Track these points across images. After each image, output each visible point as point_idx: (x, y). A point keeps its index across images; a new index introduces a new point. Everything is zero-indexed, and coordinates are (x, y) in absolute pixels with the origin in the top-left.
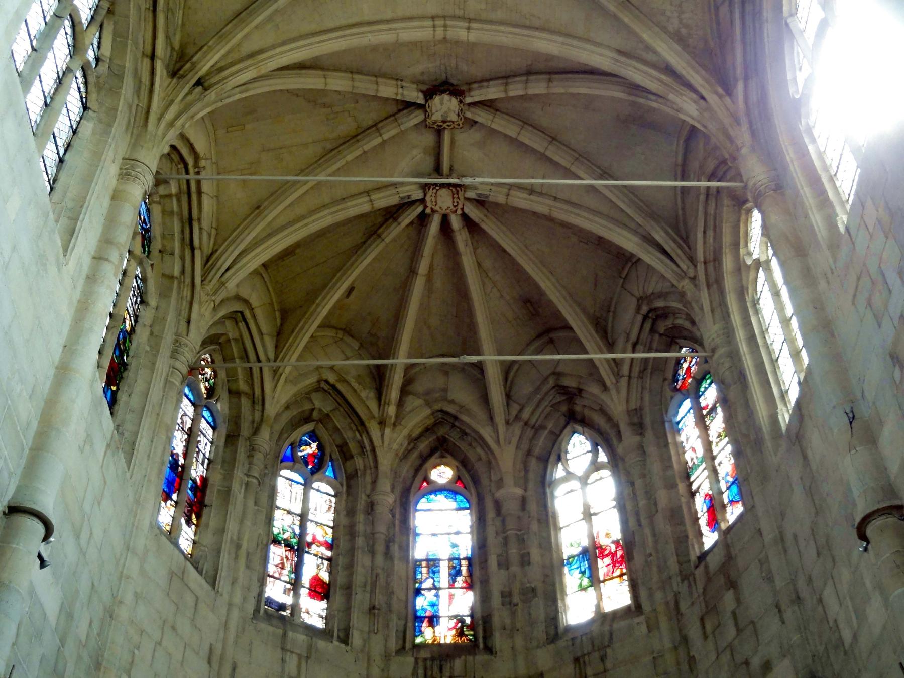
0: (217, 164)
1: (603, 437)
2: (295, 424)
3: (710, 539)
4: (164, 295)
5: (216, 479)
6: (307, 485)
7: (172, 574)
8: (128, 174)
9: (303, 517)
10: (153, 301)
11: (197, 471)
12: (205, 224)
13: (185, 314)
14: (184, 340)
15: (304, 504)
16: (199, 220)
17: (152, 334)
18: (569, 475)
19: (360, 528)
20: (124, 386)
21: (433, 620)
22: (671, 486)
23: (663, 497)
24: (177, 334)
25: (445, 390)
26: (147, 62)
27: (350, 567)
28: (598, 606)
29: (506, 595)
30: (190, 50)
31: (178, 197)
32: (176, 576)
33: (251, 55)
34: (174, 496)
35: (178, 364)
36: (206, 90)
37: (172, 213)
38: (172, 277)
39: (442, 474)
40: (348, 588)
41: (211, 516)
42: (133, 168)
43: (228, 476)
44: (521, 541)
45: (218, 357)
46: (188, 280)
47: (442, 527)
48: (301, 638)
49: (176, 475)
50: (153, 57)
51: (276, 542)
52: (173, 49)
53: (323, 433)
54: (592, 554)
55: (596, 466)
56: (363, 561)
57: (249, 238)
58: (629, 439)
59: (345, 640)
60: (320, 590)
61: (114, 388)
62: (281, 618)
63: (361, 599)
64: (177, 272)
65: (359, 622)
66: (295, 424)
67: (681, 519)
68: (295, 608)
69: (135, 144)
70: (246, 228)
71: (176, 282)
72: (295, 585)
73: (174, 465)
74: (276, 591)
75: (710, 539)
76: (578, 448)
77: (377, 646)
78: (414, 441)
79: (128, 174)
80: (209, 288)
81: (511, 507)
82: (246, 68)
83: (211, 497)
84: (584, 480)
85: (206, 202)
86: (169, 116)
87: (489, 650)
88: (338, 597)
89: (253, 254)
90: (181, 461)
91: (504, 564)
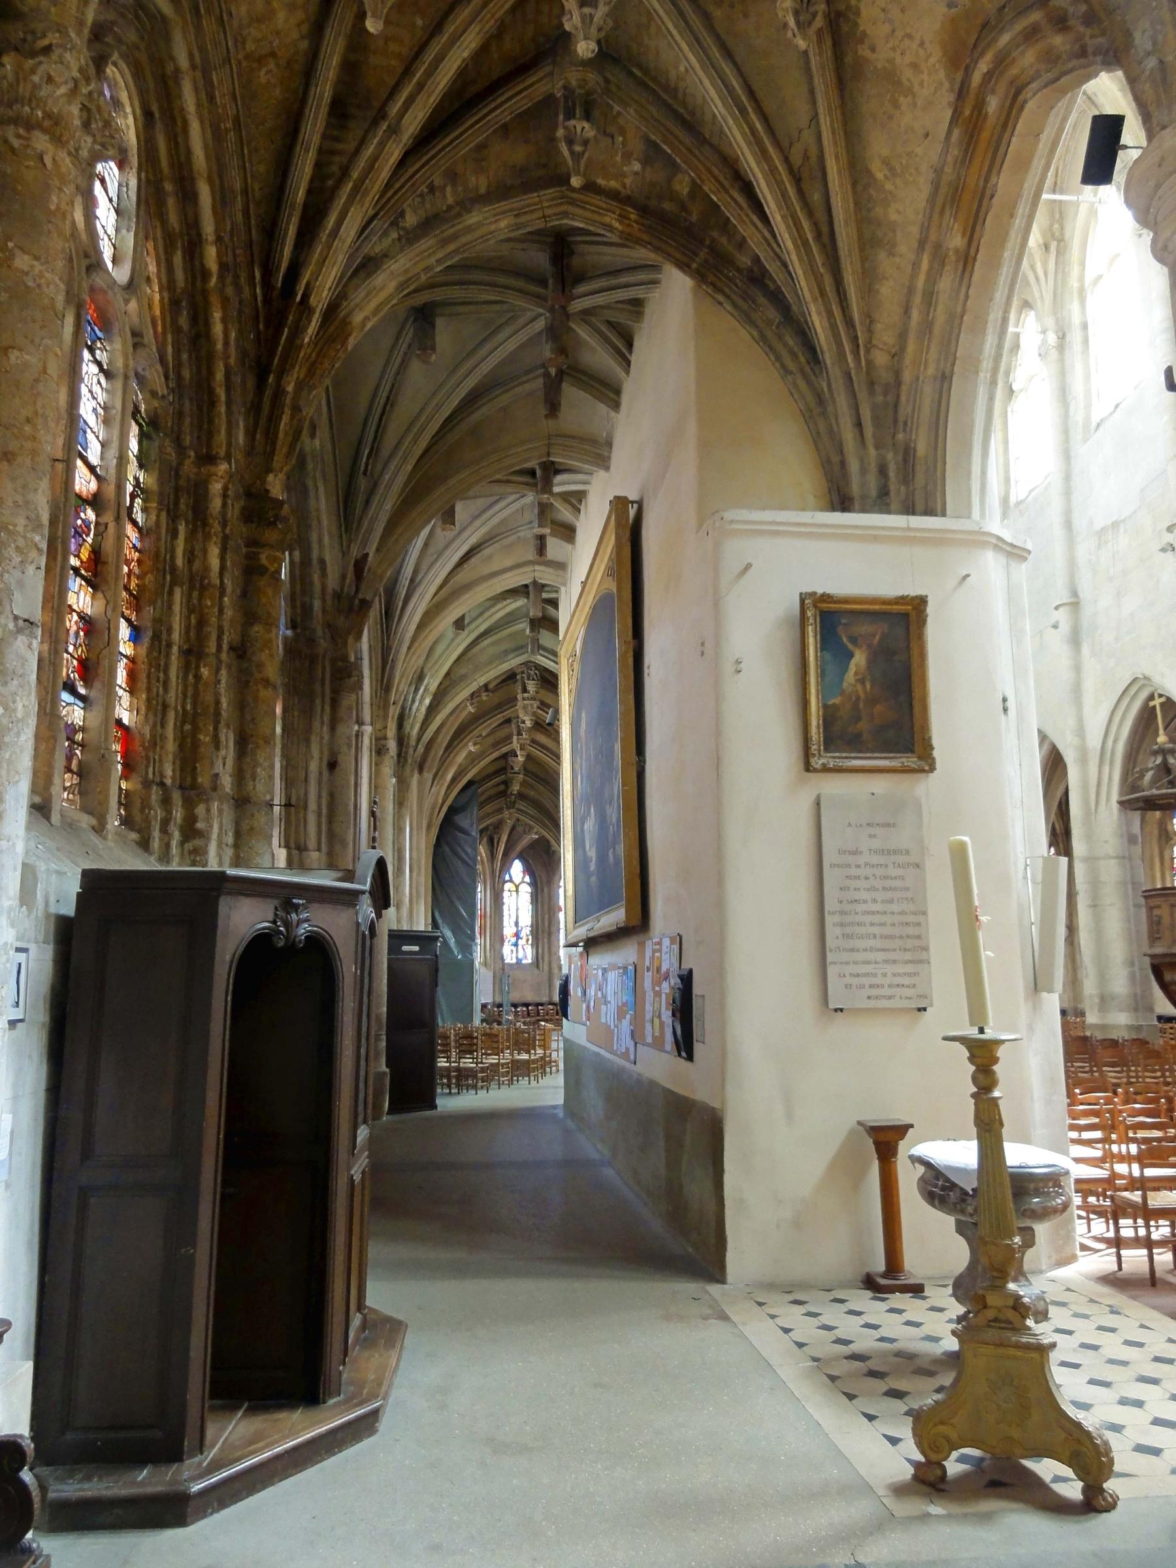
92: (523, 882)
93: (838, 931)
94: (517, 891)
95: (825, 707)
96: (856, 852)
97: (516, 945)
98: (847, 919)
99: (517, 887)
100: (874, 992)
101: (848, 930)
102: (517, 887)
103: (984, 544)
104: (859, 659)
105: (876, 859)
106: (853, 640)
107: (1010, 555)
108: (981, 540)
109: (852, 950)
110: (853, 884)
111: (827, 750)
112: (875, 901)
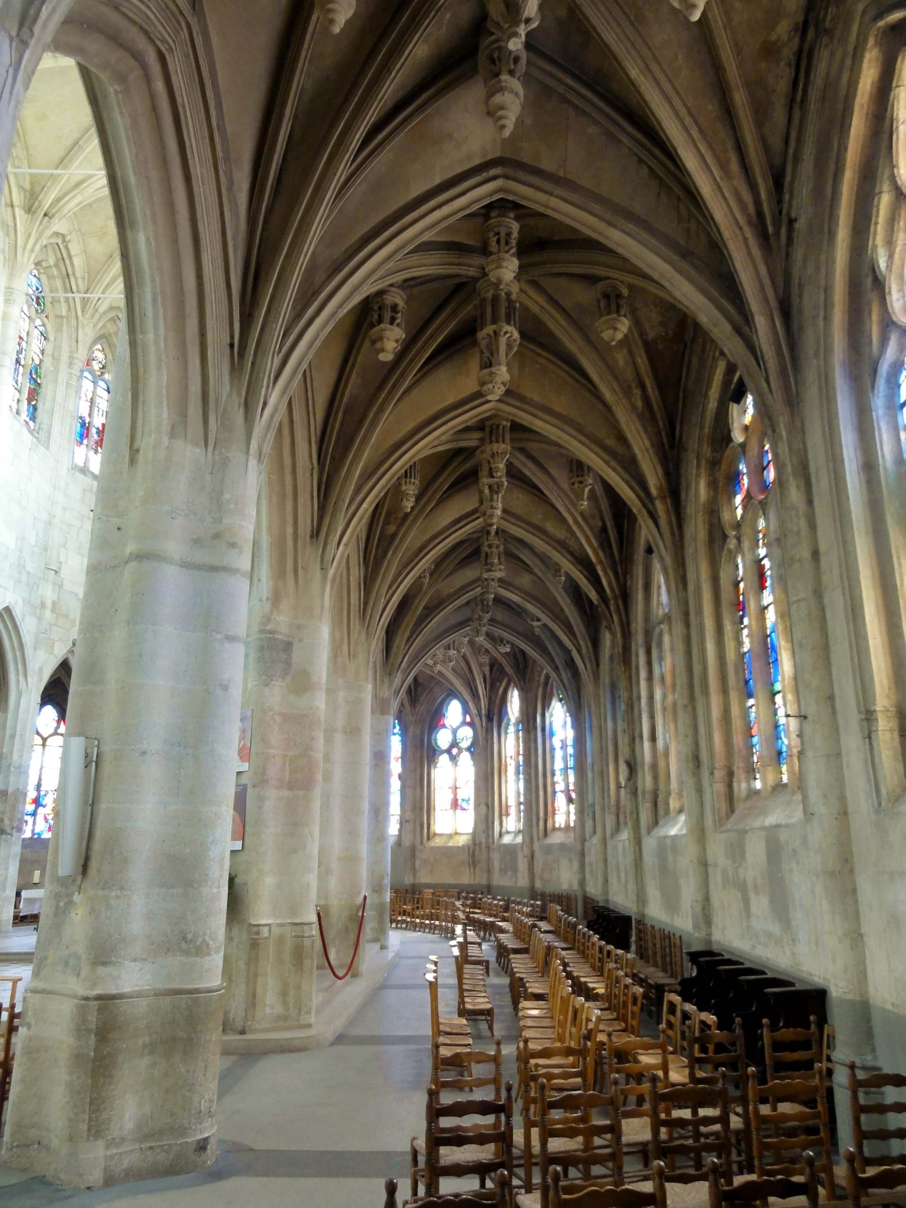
0: (80, 230)
4: (59, 329)
7: (84, 490)
8: (9, 300)
10: (51, 338)
11: (98, 421)
12: (78, 275)
13: (74, 337)
14: (76, 355)
16: (74, 274)
17: (54, 358)
20: (40, 399)
24: (71, 352)
26: (9, 210)
30: (37, 189)
31: (57, 265)
33: (78, 185)
34: (85, 442)
35: (73, 371)
36: (51, 218)
37: (54, 276)
38: (62, 317)
42: (11, 294)
45: (106, 346)
46: (73, 313)
49: (85, 429)
50: (12, 206)
52: (24, 190)
57: (110, 276)
61: (33, 403)
64: (64, 313)
69: (11, 275)
70: (106, 271)
71: (65, 320)
73: (83, 424)
79: (9, 300)
80: (87, 316)
82: (74, 196)
85: (76, 261)
86: (29, 247)
89: (113, 287)
90: (87, 420)
92: (55, 733)
94: (44, 745)
97: (34, 814)
99: (45, 740)
102: (45, 740)
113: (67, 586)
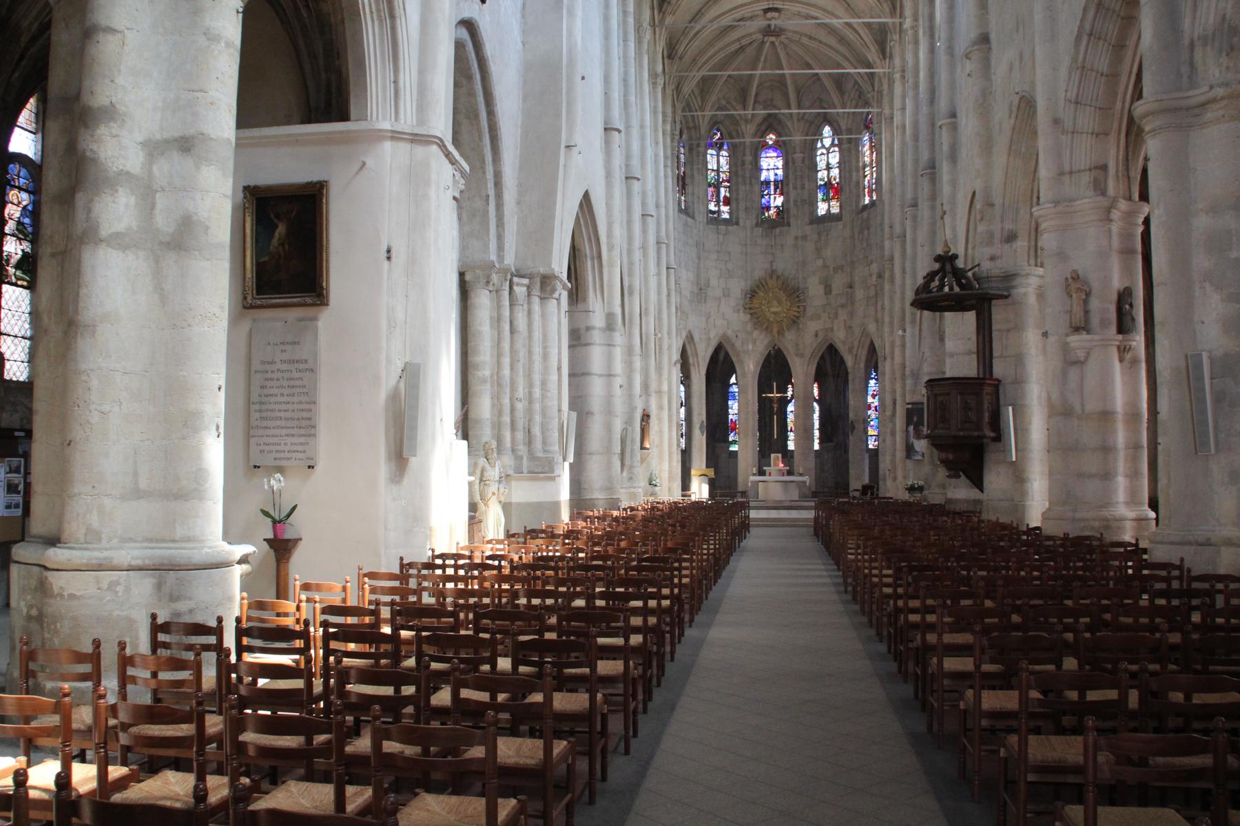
1: (836, 131)
2: (711, 129)
3: (867, 200)
5: (688, 172)
6: (718, 155)
9: (718, 171)
15: (717, 161)
18: (823, 146)
19: (740, 173)
21: (768, 208)
22: (858, 171)
23: (854, 174)
25: (772, 100)
27: (737, 190)
28: (829, 210)
29: (795, 201)
32: (686, 224)
39: (771, 138)
40: (737, 200)
41: (689, 189)
43: (692, 169)
44: (802, 177)
47: (771, 165)
48: (723, 228)
51: (710, 185)
53: (721, 127)
54: (828, 185)
55: (833, 145)
56: (742, 188)
58: (845, 146)
59: (737, 224)
60: (727, 202)
62: (714, 219)
63: (742, 205)
65: (742, 215)
66: (711, 129)
67: (859, 185)
68: (719, 212)
72: (718, 201)
74: (712, 207)
75: (867, 200)
76: (827, 131)
77: (748, 224)
78: (760, 125)
81: (799, 163)
83: (688, 180)
84: (828, 150)
87: (789, 225)
88: (734, 204)
91: (795, 188)
93: (257, 415)
95: (258, 264)
96: (273, 362)
98: (264, 407)
100: (278, 455)
101: (264, 414)
103: (383, 138)
104: (281, 229)
105: (285, 367)
106: (278, 216)
107: (412, 141)
108: (378, 136)
109: (266, 428)
110: (269, 383)
111: (258, 294)
112: (282, 395)
113: (684, 292)
